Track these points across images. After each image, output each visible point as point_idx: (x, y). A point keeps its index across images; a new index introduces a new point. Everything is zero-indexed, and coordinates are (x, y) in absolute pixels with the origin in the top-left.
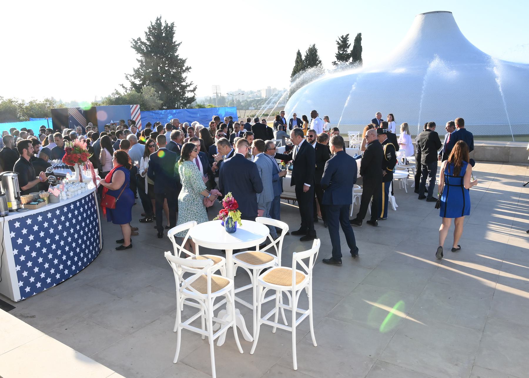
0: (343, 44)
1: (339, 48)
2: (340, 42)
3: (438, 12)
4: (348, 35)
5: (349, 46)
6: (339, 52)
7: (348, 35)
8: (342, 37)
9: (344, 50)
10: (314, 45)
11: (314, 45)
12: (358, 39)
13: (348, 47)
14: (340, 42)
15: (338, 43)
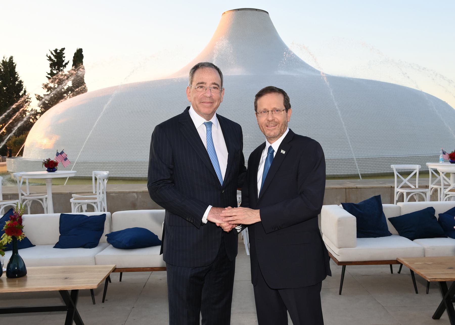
0: (57, 60)
1: (51, 66)
2: (53, 58)
3: (256, 10)
4: (63, 49)
5: (67, 64)
6: (51, 71)
7: (63, 49)
8: (56, 51)
9: (59, 69)
10: (11, 58)
11: (11, 58)
12: (79, 57)
13: (65, 66)
14: (53, 58)
15: (50, 59)
